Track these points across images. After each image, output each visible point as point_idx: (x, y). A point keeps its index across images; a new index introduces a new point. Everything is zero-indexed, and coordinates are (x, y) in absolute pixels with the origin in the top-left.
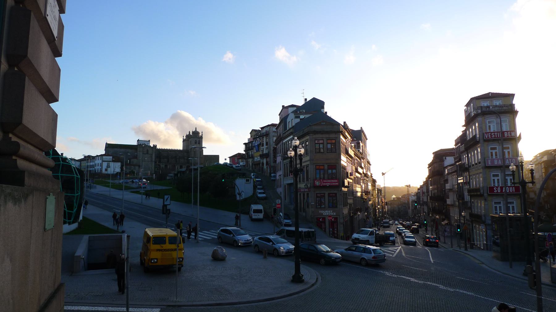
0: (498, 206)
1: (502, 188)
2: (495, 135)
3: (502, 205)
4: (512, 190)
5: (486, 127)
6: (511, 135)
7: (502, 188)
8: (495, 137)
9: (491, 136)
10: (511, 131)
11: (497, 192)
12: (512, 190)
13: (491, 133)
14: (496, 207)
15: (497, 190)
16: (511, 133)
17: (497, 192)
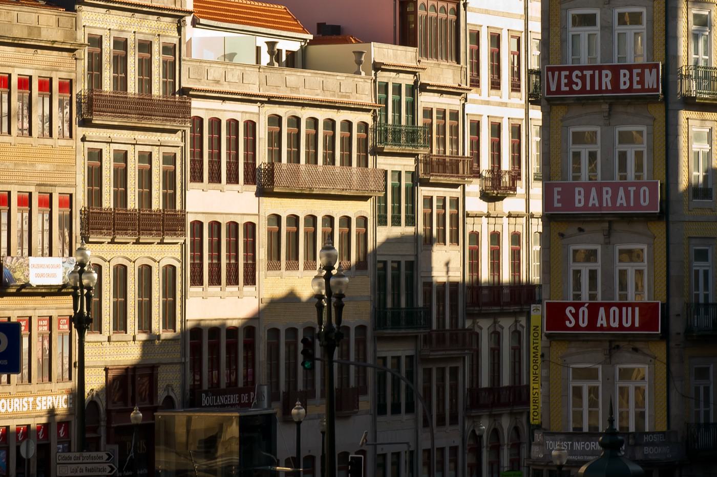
0: (585, 386)
1: (593, 310)
2: (583, 78)
3: (599, 384)
4: (632, 319)
5: (563, 41)
6: (641, 82)
7: (593, 310)
8: (583, 90)
9: (570, 83)
10: (642, 67)
11: (577, 327)
12: (632, 319)
13: (571, 69)
14: (578, 392)
15: (576, 316)
16: (641, 75)
17: (577, 327)
